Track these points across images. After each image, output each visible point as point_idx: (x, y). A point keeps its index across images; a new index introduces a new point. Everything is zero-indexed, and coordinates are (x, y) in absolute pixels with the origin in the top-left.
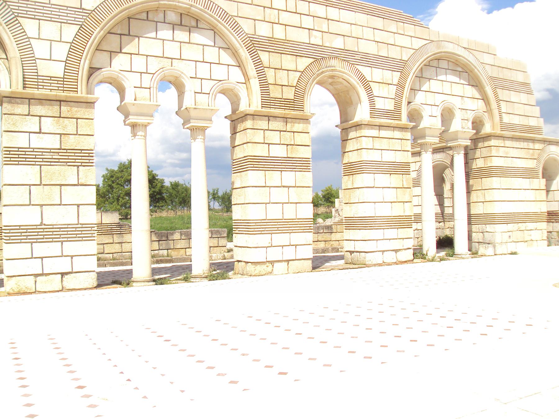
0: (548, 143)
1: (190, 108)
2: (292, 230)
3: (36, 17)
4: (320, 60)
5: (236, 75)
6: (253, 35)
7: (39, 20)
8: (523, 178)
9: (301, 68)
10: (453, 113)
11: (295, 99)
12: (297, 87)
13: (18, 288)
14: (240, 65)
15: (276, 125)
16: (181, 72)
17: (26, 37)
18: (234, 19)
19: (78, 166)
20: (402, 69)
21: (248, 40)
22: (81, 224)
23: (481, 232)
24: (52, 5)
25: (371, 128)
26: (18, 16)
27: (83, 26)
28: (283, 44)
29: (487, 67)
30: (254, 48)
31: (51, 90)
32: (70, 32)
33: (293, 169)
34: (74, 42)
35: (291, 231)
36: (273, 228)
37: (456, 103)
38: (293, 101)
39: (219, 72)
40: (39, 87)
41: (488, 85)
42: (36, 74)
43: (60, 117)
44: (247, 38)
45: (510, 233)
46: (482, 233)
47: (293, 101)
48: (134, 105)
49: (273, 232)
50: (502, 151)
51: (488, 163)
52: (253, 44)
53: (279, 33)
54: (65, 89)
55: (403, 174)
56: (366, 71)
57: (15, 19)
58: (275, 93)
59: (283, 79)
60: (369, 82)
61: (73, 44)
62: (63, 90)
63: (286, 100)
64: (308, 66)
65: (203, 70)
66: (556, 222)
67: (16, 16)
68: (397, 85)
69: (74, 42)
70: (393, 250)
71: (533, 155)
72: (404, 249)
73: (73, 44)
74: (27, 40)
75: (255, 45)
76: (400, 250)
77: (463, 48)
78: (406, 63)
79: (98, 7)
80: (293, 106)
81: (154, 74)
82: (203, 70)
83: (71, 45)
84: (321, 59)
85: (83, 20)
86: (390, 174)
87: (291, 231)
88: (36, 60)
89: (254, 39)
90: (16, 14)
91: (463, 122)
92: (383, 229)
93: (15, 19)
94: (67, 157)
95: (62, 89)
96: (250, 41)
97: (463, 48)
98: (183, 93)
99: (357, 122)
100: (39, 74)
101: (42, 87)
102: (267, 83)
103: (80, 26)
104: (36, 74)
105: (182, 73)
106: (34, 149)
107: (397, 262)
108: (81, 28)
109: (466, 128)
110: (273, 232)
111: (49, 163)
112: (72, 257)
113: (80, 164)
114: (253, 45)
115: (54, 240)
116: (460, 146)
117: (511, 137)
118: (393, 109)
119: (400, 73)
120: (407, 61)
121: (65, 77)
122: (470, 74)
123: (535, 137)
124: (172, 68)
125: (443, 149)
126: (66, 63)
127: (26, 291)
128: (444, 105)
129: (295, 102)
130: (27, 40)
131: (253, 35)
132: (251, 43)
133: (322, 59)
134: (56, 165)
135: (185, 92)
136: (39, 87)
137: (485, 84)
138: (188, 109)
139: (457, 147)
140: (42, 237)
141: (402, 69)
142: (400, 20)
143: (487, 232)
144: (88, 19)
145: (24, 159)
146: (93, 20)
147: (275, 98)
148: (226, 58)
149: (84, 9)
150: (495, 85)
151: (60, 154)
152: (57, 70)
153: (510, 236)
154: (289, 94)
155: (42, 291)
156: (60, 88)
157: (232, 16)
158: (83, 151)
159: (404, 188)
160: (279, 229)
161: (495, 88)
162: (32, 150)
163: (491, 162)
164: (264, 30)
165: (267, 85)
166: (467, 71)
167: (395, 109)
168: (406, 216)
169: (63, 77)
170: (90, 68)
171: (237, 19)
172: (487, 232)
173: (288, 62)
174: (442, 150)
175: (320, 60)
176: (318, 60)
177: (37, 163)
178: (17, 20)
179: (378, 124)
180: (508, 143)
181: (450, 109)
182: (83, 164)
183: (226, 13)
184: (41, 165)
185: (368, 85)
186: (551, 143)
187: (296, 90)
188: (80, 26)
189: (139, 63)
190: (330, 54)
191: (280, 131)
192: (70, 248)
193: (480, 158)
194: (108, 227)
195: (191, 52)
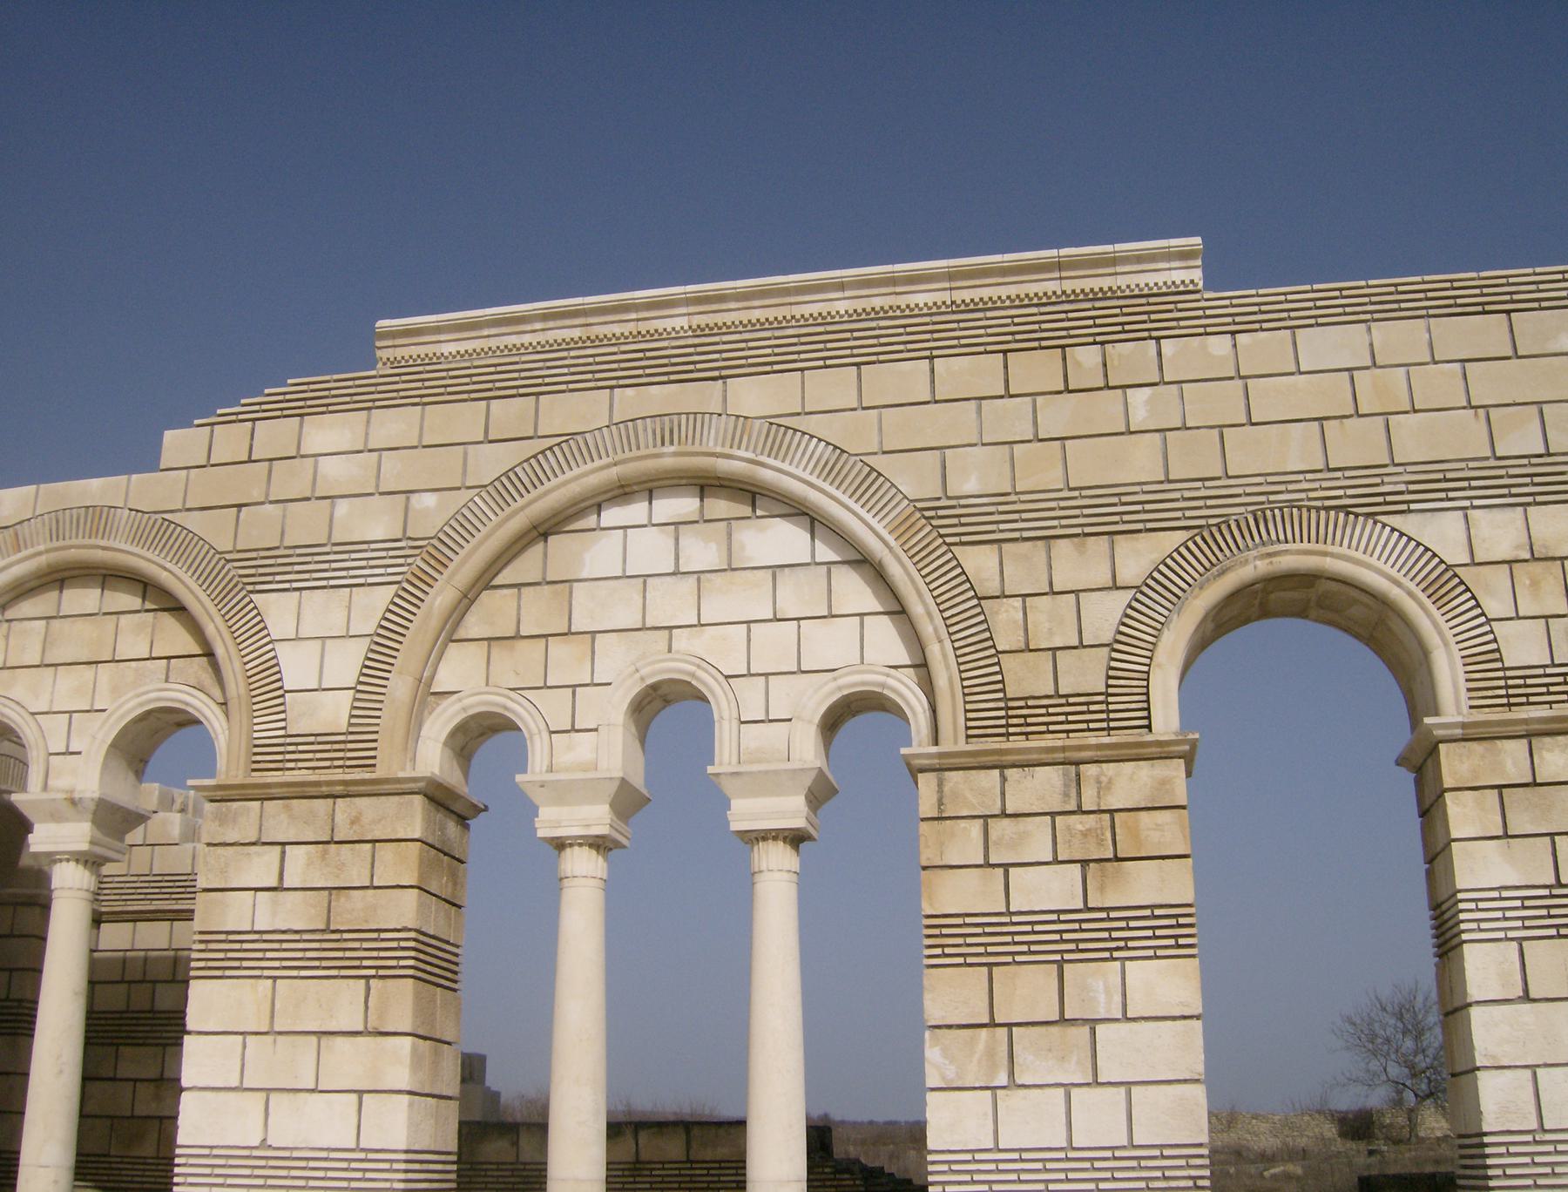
4: (1214, 529)
5: (886, 643)
22: (363, 1150)
26: (251, 592)
33: (1116, 950)
48: (542, 786)
65: (774, 646)
67: (251, 592)
75: (942, 531)
82: (774, 646)
84: (1218, 525)
90: (250, 588)
94: (299, 955)
113: (373, 972)
124: (670, 655)
148: (855, 592)
152: (333, 713)
154: (1085, 675)
171: (876, 462)
175: (1214, 529)
182: (381, 972)
184: (275, 978)
190: (1262, 498)
191: (1053, 814)
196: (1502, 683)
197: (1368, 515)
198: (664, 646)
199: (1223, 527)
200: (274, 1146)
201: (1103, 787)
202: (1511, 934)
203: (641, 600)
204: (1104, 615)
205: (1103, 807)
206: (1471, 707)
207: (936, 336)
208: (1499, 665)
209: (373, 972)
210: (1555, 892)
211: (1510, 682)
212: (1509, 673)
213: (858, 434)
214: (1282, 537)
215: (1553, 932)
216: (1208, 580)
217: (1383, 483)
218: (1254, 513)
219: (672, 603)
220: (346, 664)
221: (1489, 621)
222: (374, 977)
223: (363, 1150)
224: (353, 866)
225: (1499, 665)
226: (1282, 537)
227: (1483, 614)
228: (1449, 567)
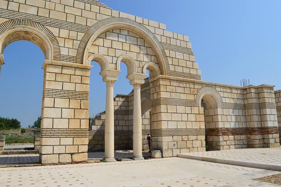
0: (205, 85)
25: (55, 67)
37: (133, 56)
56: (55, 31)
71: (193, 92)
76: (75, 153)
91: (139, 69)
109: (140, 72)
116: (136, 84)
117: (176, 79)
119: (84, 34)
123: (195, 81)
141: (86, 31)
166: (143, 38)
175: (14, 20)
179: (61, 65)
186: (207, 85)
196: (59, 57)
197: (43, 25)
202: (53, 97)
206: (54, 59)
208: (60, 54)
210: (62, 91)
211: (61, 57)
212: (61, 55)
214: (26, 24)
215: (60, 97)
216: (11, 28)
217: (46, 20)
221: (59, 47)
225: (60, 54)
226: (26, 24)
227: (59, 45)
228: (55, 37)
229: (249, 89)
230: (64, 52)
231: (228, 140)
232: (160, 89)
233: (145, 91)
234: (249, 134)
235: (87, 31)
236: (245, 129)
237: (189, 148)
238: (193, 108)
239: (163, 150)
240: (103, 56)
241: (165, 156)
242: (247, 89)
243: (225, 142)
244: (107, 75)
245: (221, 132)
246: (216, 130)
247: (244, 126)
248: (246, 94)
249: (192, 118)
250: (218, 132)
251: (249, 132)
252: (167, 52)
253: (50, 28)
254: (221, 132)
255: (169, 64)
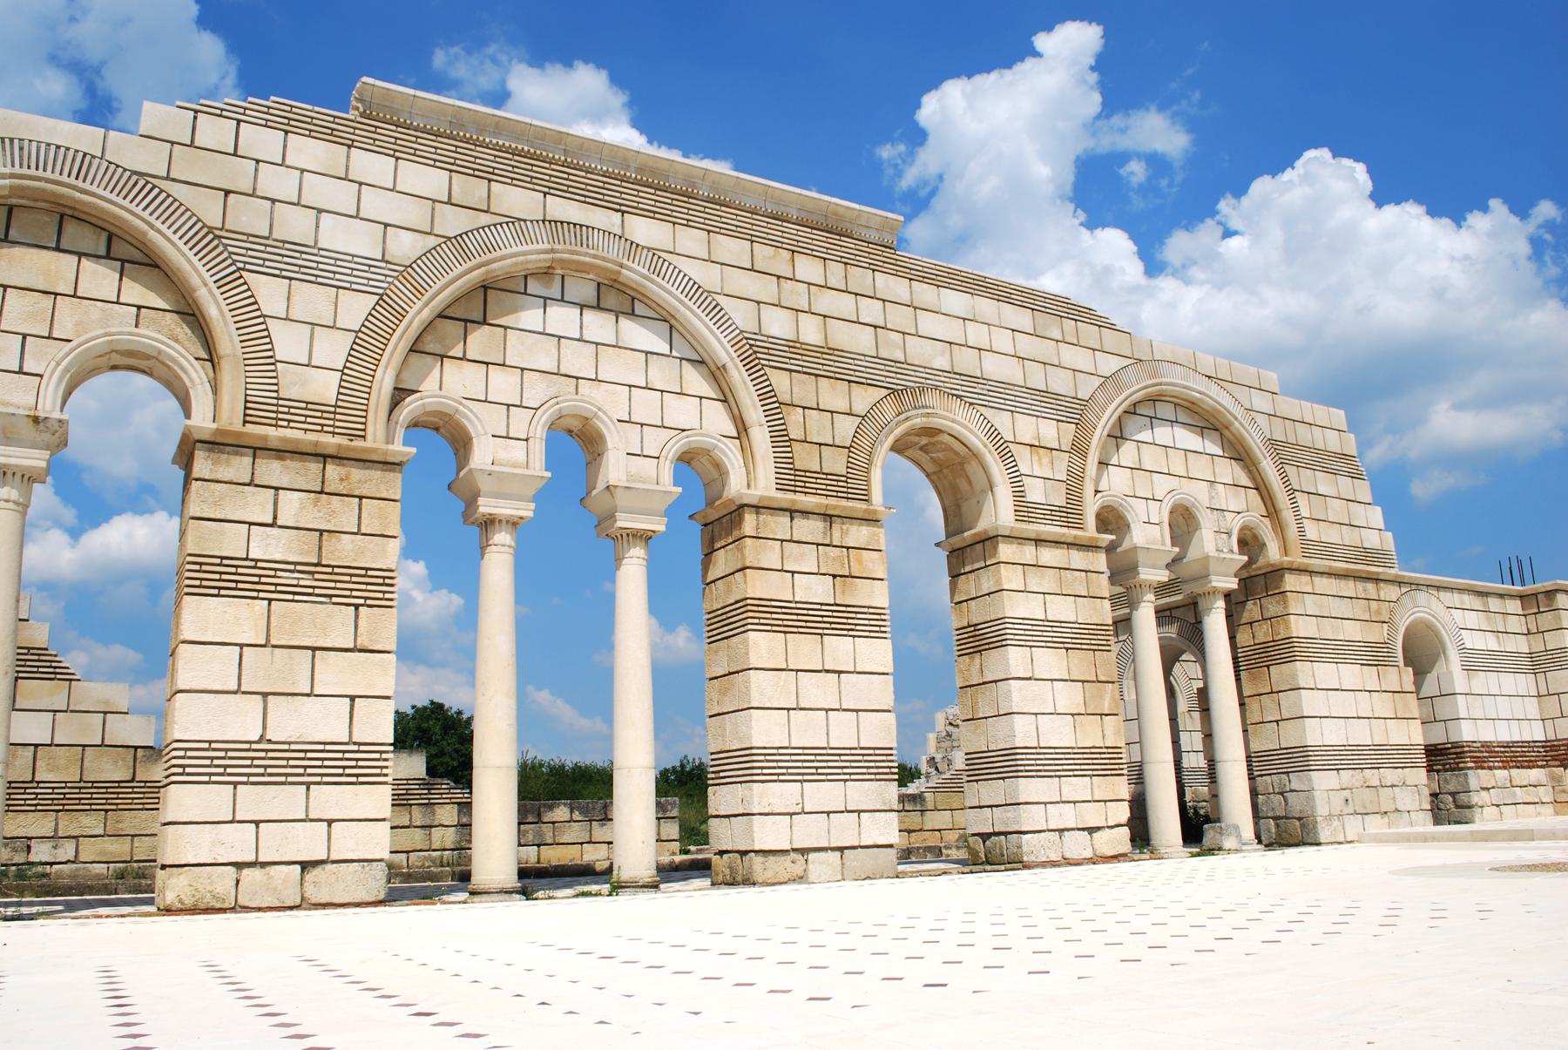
1: (616, 487)
2: (850, 774)
3: (284, 273)
4: (900, 392)
5: (718, 421)
6: (755, 334)
7: (291, 279)
8: (1362, 664)
9: (860, 407)
10: (1193, 517)
11: (849, 475)
12: (852, 449)
13: (194, 896)
14: (726, 397)
15: (809, 528)
16: (596, 407)
17: (258, 313)
18: (714, 300)
19: (357, 606)
20: (1078, 417)
21: (745, 345)
22: (355, 743)
23: (1278, 793)
24: (320, 249)
26: (243, 269)
27: (385, 297)
28: (819, 355)
29: (1259, 418)
30: (757, 361)
31: (306, 430)
32: (355, 309)
33: (849, 631)
34: (363, 329)
35: (847, 777)
36: (804, 768)
37: (1198, 494)
38: (844, 479)
39: (682, 412)
40: (280, 423)
41: (1265, 458)
42: (275, 395)
43: (321, 492)
44: (742, 339)
45: (1346, 793)
46: (1282, 794)
47: (844, 479)
48: (490, 474)
49: (806, 777)
50: (1311, 603)
51: (1282, 631)
52: (755, 352)
53: (811, 332)
54: (337, 430)
55: (1094, 650)
56: (1002, 421)
57: (237, 275)
58: (806, 459)
59: (818, 427)
60: (1010, 444)
61: (360, 335)
62: (333, 433)
63: (829, 477)
64: (875, 405)
65: (646, 406)
66: (1446, 770)
67: (239, 269)
68: (1070, 452)
69: (363, 329)
70: (1083, 829)
71: (1378, 612)
72: (1108, 827)
73: (360, 335)
74: (261, 320)
75: (759, 355)
77: (1206, 376)
78: (1085, 406)
79: (420, 258)
80: (845, 490)
81: (537, 409)
82: (646, 406)
83: (357, 337)
84: (902, 390)
85: (385, 285)
86: (1067, 649)
87: (847, 777)
88: (278, 364)
89: (758, 343)
90: (241, 265)
91: (1218, 537)
92: (1056, 776)
93: (237, 275)
95: (331, 429)
96: (748, 346)
97: (1206, 376)
98: (599, 455)
99: (986, 532)
100: (281, 396)
101: (285, 423)
102: (787, 438)
103: (378, 297)
104: (275, 395)
105: (600, 409)
106: (256, 561)
107: (1095, 858)
108: (381, 302)
109: (1225, 550)
110: (806, 777)
111: (290, 597)
112: (330, 822)
113: (362, 601)
114: (754, 356)
115: (290, 779)
116: (1214, 593)
117: (1326, 571)
118: (1065, 505)
119: (1074, 425)
120: (1087, 401)
121: (339, 403)
122: (1226, 432)
123: (1378, 573)
124: (576, 397)
125: (1170, 609)
126: (343, 374)
127: (211, 904)
128: (1173, 499)
129: (849, 480)
130: (261, 320)
131: (755, 334)
132: (751, 351)
133: (904, 392)
134: (306, 602)
135: (603, 454)
136: (280, 423)
137: (1261, 457)
138: (611, 488)
139: (1209, 593)
140: (261, 770)
141: (1078, 417)
142: (1068, 313)
143: (1292, 791)
144: (396, 282)
145: (233, 585)
146: (408, 286)
147: (805, 471)
148: (697, 382)
149: (387, 262)
150: (1280, 458)
151: (316, 576)
152: (324, 387)
153: (1347, 800)
154: (836, 463)
155: (251, 906)
156: (326, 429)
157: (708, 292)
158: (370, 573)
159: (1099, 682)
160: (820, 771)
161: (1281, 463)
162: (252, 564)
163: (1288, 628)
164: (778, 325)
165: (787, 441)
167: (1067, 503)
168: (1107, 748)
169: (334, 404)
170: (395, 388)
171: (721, 300)
172: (1292, 791)
173: (833, 395)
174: (1168, 612)
176: (896, 393)
177: (262, 595)
178: (241, 277)
179: (1033, 536)
180: (1323, 584)
181: (1187, 509)
182: (369, 602)
183: (696, 286)
184: (270, 600)
185: (1007, 450)
187: (851, 454)
188: (378, 297)
189: (503, 384)
190: (923, 381)
191: (818, 545)
192: (330, 800)
193: (1259, 621)
194: (400, 787)
195: (615, 367)
197: (971, 404)
198: (573, 389)
199: (904, 392)
200: (273, 740)
201: (844, 534)
203: (557, 353)
204: (846, 427)
205: (844, 545)
207: (739, 229)
209: (362, 601)
213: (706, 276)
218: (923, 388)
219: (577, 360)
220: (333, 349)
222: (362, 605)
223: (355, 743)
224: (343, 514)
229: (1545, 597)
230: (1036, 493)
231: (1493, 788)
232: (1285, 608)
233: (1168, 613)
234: (1558, 763)
235: (1075, 412)
236: (1543, 747)
237: (1386, 813)
238: (1382, 670)
239: (1319, 819)
240: (1126, 498)
241: (1326, 838)
242: (1539, 596)
243: (1484, 793)
244: (618, 509)
245: (1470, 757)
246: (1453, 750)
247: (1539, 736)
248: (1535, 614)
249: (1383, 706)
250: (1460, 755)
251: (1554, 758)
252: (1291, 470)
253: (988, 413)
254: (1470, 757)
255: (1303, 515)
